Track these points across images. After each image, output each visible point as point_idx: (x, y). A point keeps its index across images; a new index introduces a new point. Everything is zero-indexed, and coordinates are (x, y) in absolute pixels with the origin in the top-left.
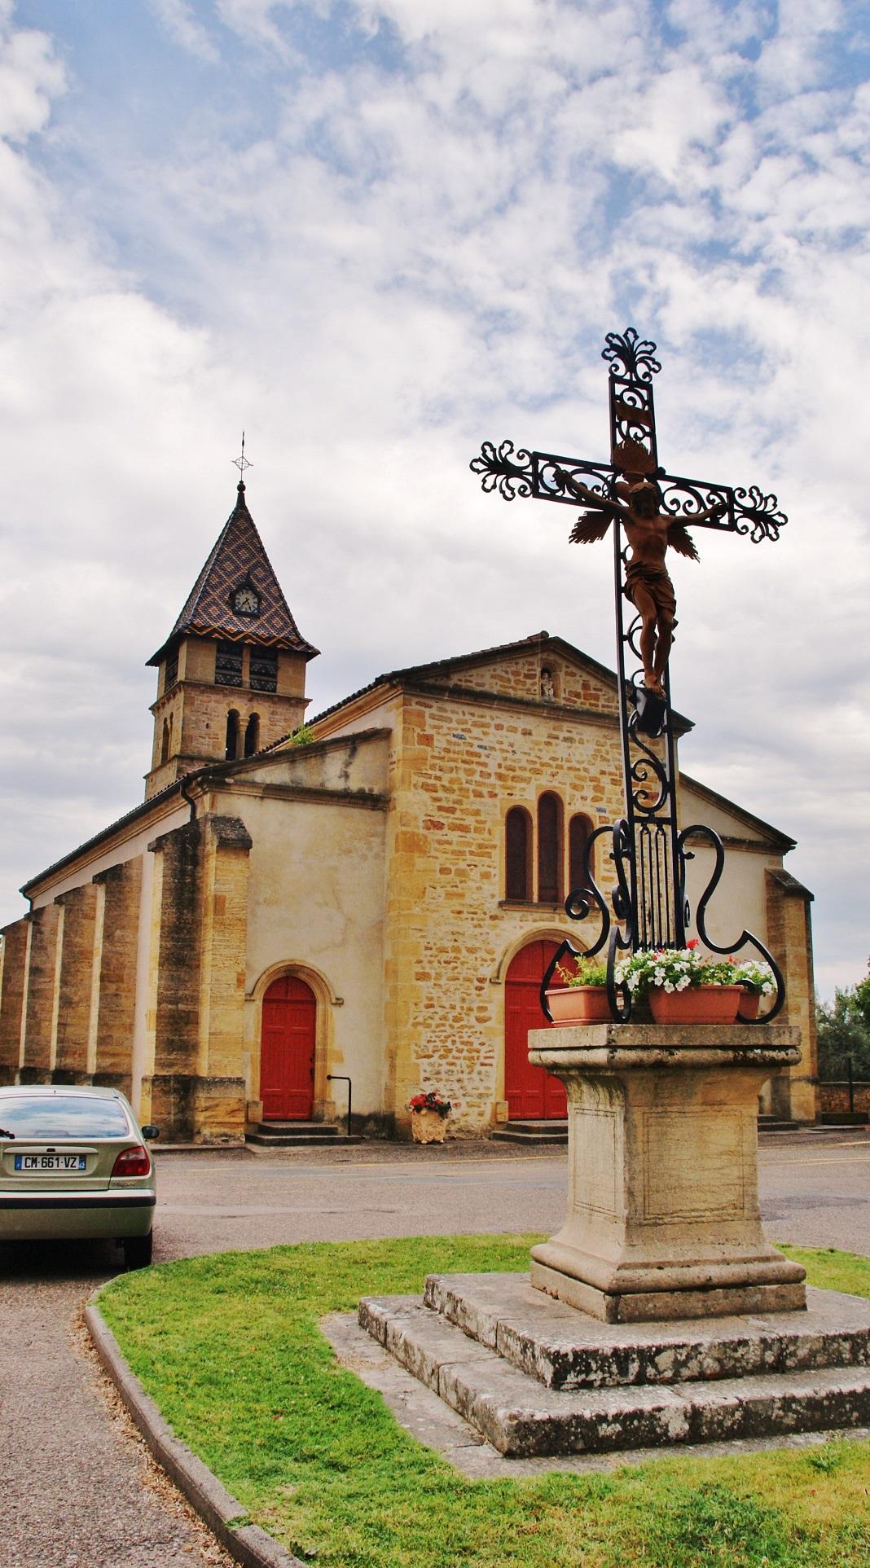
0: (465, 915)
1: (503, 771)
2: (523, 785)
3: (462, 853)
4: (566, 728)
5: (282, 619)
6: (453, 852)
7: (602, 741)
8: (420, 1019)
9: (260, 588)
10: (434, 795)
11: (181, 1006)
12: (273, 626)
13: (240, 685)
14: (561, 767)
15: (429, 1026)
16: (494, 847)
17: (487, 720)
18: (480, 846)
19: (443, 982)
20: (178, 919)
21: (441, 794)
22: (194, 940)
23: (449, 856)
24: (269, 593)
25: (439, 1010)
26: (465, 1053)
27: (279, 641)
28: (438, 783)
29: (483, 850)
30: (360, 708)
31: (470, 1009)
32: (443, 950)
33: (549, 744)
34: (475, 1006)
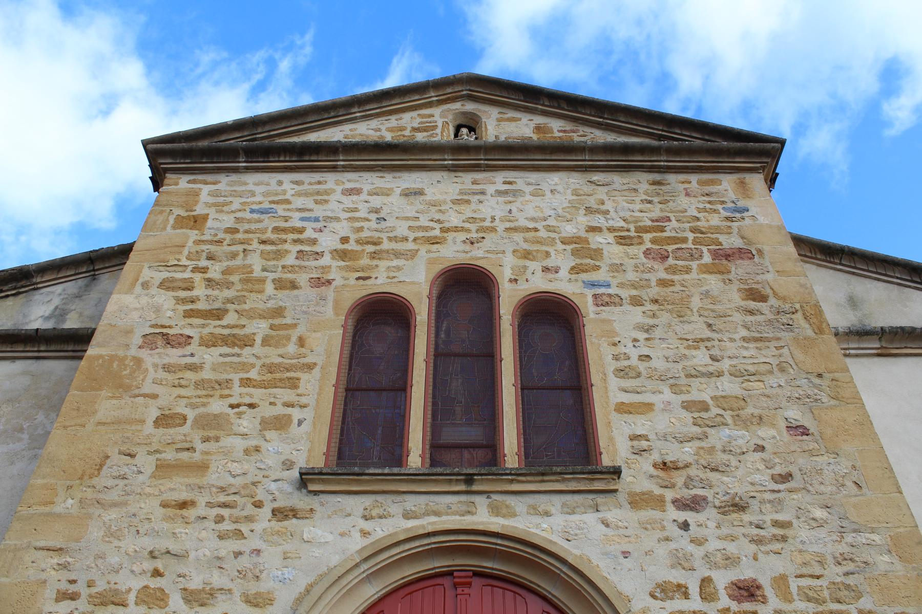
0: (201, 510)
1: (352, 246)
7: (588, 189)
14: (493, 230)
16: (310, 367)
17: (330, 185)
18: (270, 368)
29: (281, 377)
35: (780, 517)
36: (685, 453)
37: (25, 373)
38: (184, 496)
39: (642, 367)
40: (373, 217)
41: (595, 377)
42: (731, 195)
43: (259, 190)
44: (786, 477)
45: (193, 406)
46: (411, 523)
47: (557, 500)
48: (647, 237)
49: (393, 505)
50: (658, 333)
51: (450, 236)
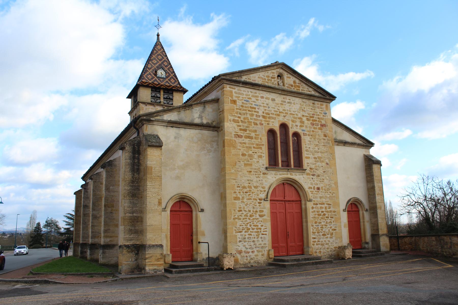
2: (273, 120)
3: (250, 147)
4: (288, 98)
5: (174, 79)
6: (247, 147)
7: (302, 103)
8: (236, 217)
9: (166, 69)
10: (238, 124)
11: (134, 214)
12: (171, 82)
13: (160, 102)
15: (240, 219)
16: (263, 145)
17: (257, 94)
18: (257, 145)
19: (245, 200)
20: (133, 177)
21: (240, 124)
22: (139, 186)
23: (245, 149)
24: (169, 70)
25: (244, 212)
26: (255, 230)
27: (173, 87)
28: (239, 119)
29: (259, 146)
30: (206, 92)
31: (256, 211)
32: (244, 187)
33: (281, 104)
34: (258, 210)
36: (313, 166)
37: (199, 133)
38: (250, 170)
39: (309, 149)
40: (267, 106)
41: (303, 151)
42: (325, 109)
43: (245, 93)
44: (324, 172)
45: (247, 152)
46: (281, 176)
47: (298, 173)
48: (311, 119)
49: (279, 173)
50: (311, 143)
51: (281, 114)
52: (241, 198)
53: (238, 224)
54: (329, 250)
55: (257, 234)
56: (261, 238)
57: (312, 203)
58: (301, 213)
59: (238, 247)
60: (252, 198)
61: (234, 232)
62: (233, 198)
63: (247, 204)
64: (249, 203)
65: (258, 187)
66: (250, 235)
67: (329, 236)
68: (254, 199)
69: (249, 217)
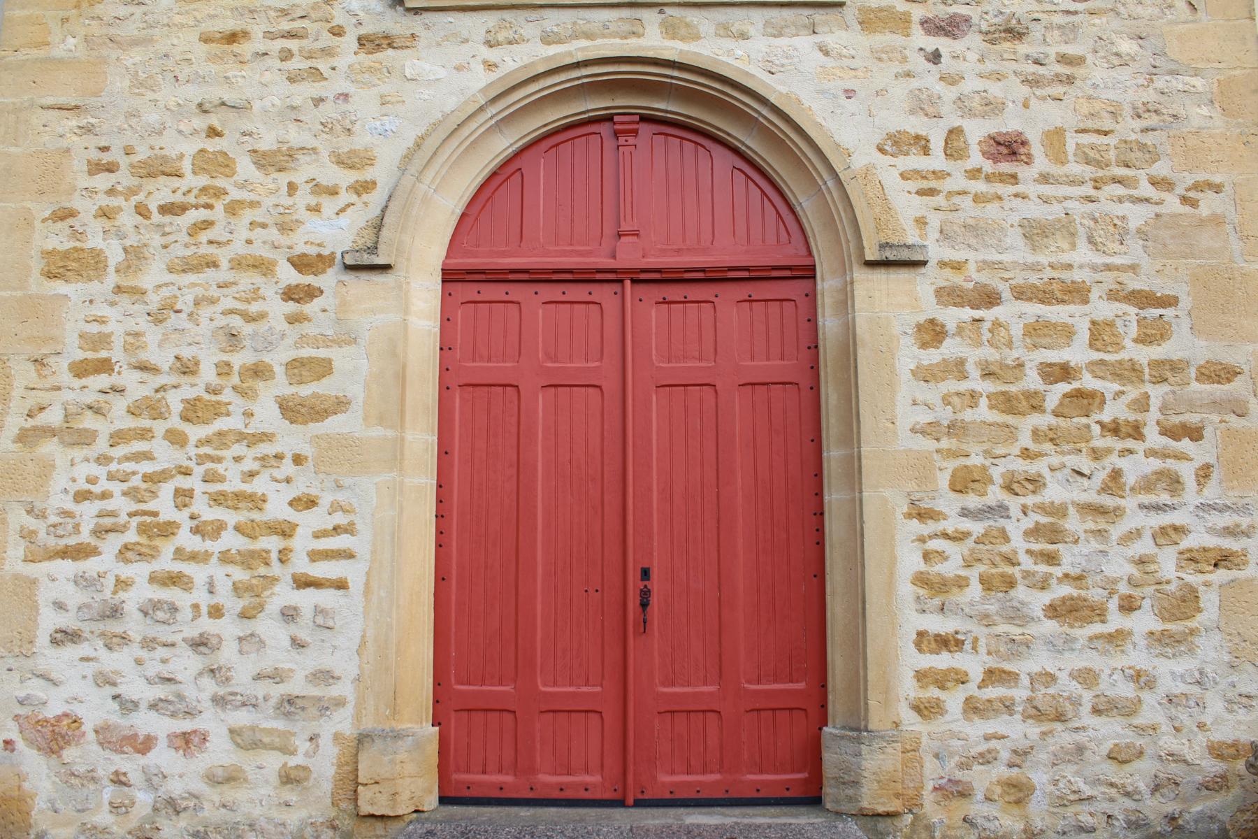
0: (258, 44)
8: (53, 417)
15: (85, 438)
19: (152, 276)
25: (129, 378)
26: (230, 541)
32: (162, 168)
34: (277, 359)
35: (1070, 50)
46: (552, 50)
52: (114, 254)
53: (59, 481)
54: (1139, 775)
55: (240, 574)
56: (289, 615)
57: (923, 285)
58: (815, 388)
59: (36, 688)
60: (223, 256)
61: (16, 551)
62: (37, 265)
63: (169, 307)
64: (185, 302)
65: (291, 155)
66: (173, 580)
67: (1144, 622)
68: (238, 264)
69: (174, 422)
